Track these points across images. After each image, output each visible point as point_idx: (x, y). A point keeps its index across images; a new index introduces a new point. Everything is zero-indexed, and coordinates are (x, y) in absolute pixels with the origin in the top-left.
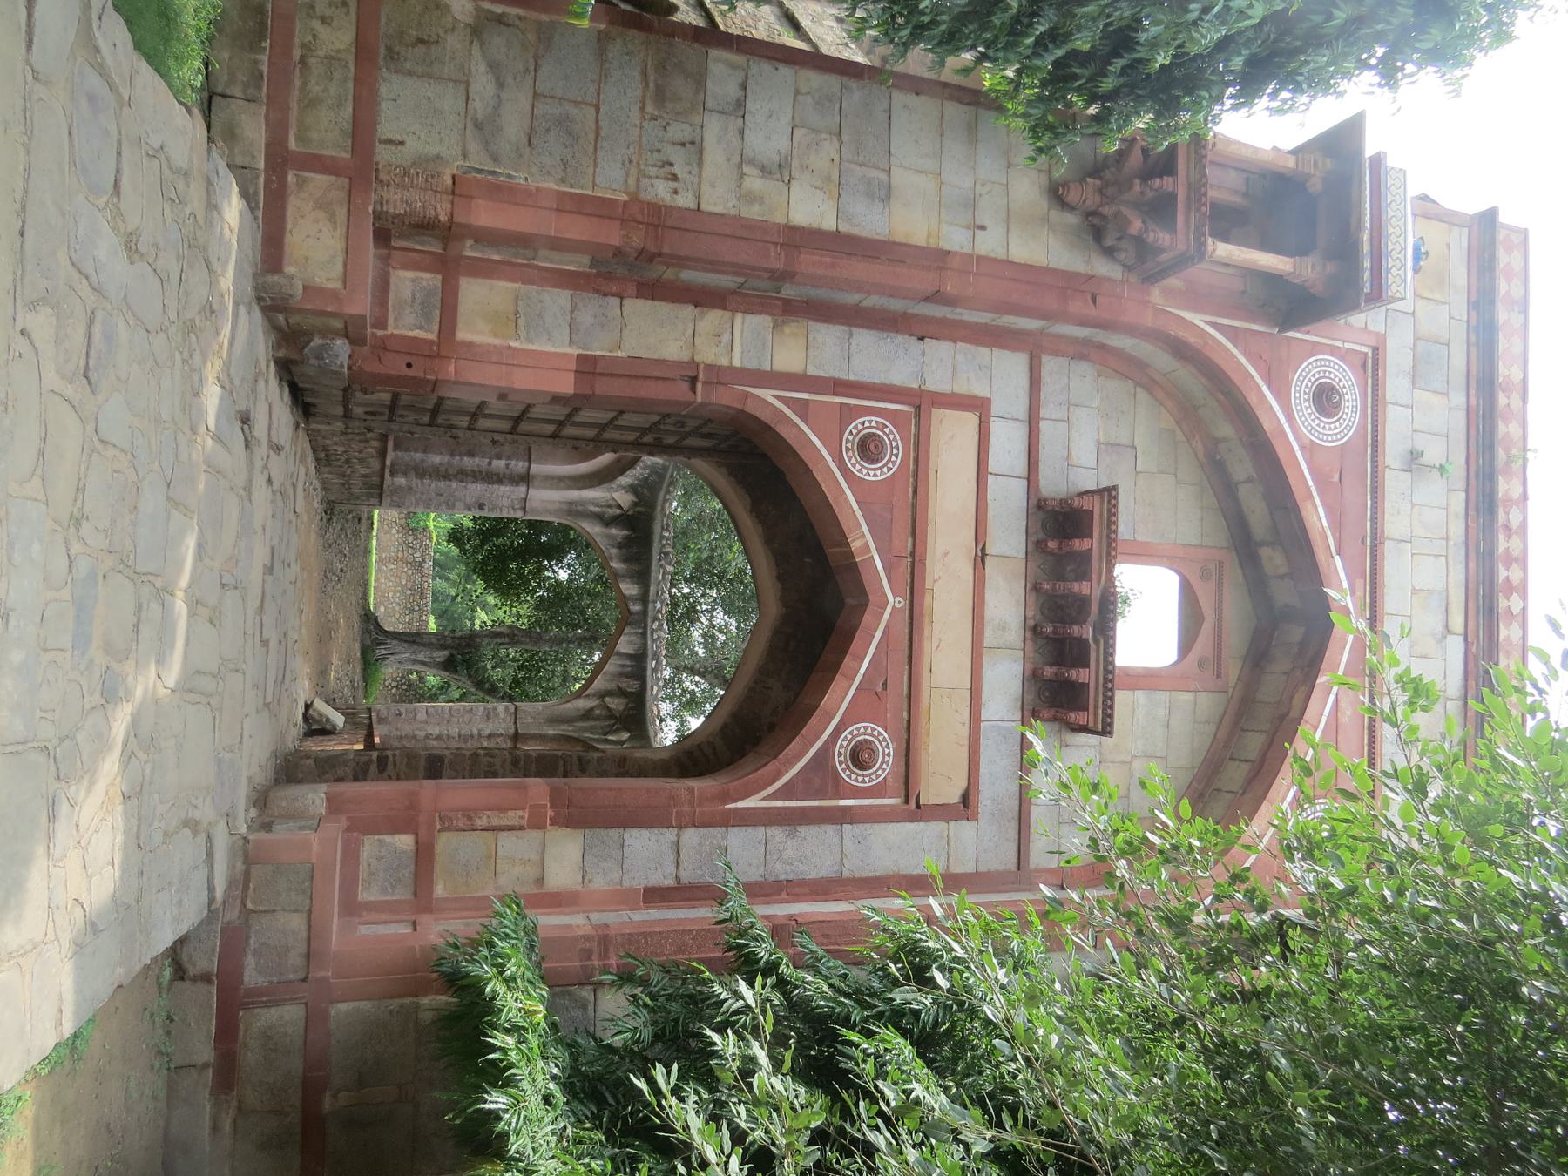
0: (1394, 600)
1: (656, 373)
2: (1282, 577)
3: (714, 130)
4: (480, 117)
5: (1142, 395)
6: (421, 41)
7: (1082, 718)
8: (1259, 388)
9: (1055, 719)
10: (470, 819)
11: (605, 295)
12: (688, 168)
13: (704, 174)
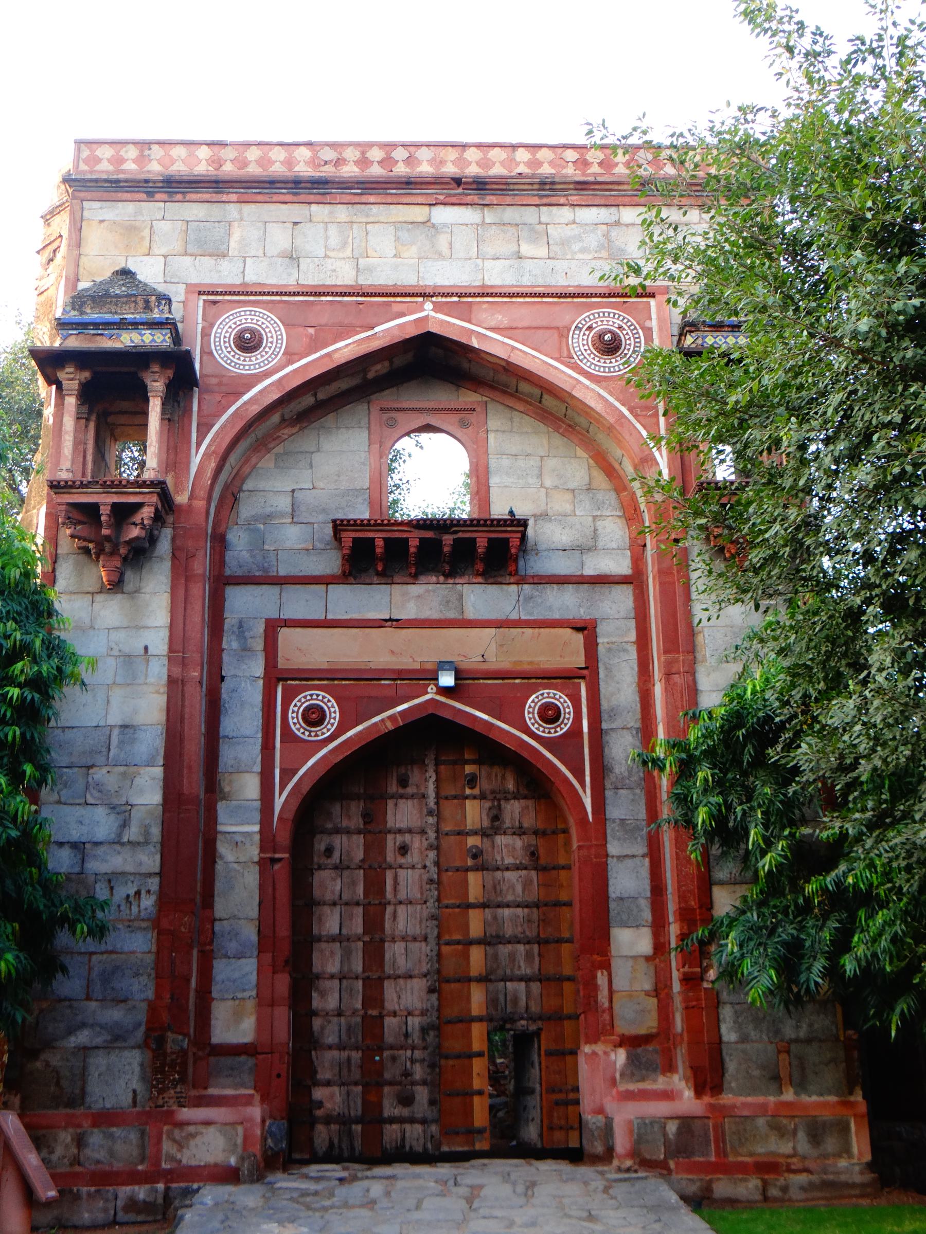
0: (407, 279)
1: (270, 890)
2: (391, 363)
3: (95, 866)
4: (109, 1038)
5: (249, 485)
6: (58, 1084)
7: (515, 542)
8: (245, 403)
9: (516, 560)
10: (604, 1011)
11: (213, 933)
12: (129, 883)
13: (132, 871)
